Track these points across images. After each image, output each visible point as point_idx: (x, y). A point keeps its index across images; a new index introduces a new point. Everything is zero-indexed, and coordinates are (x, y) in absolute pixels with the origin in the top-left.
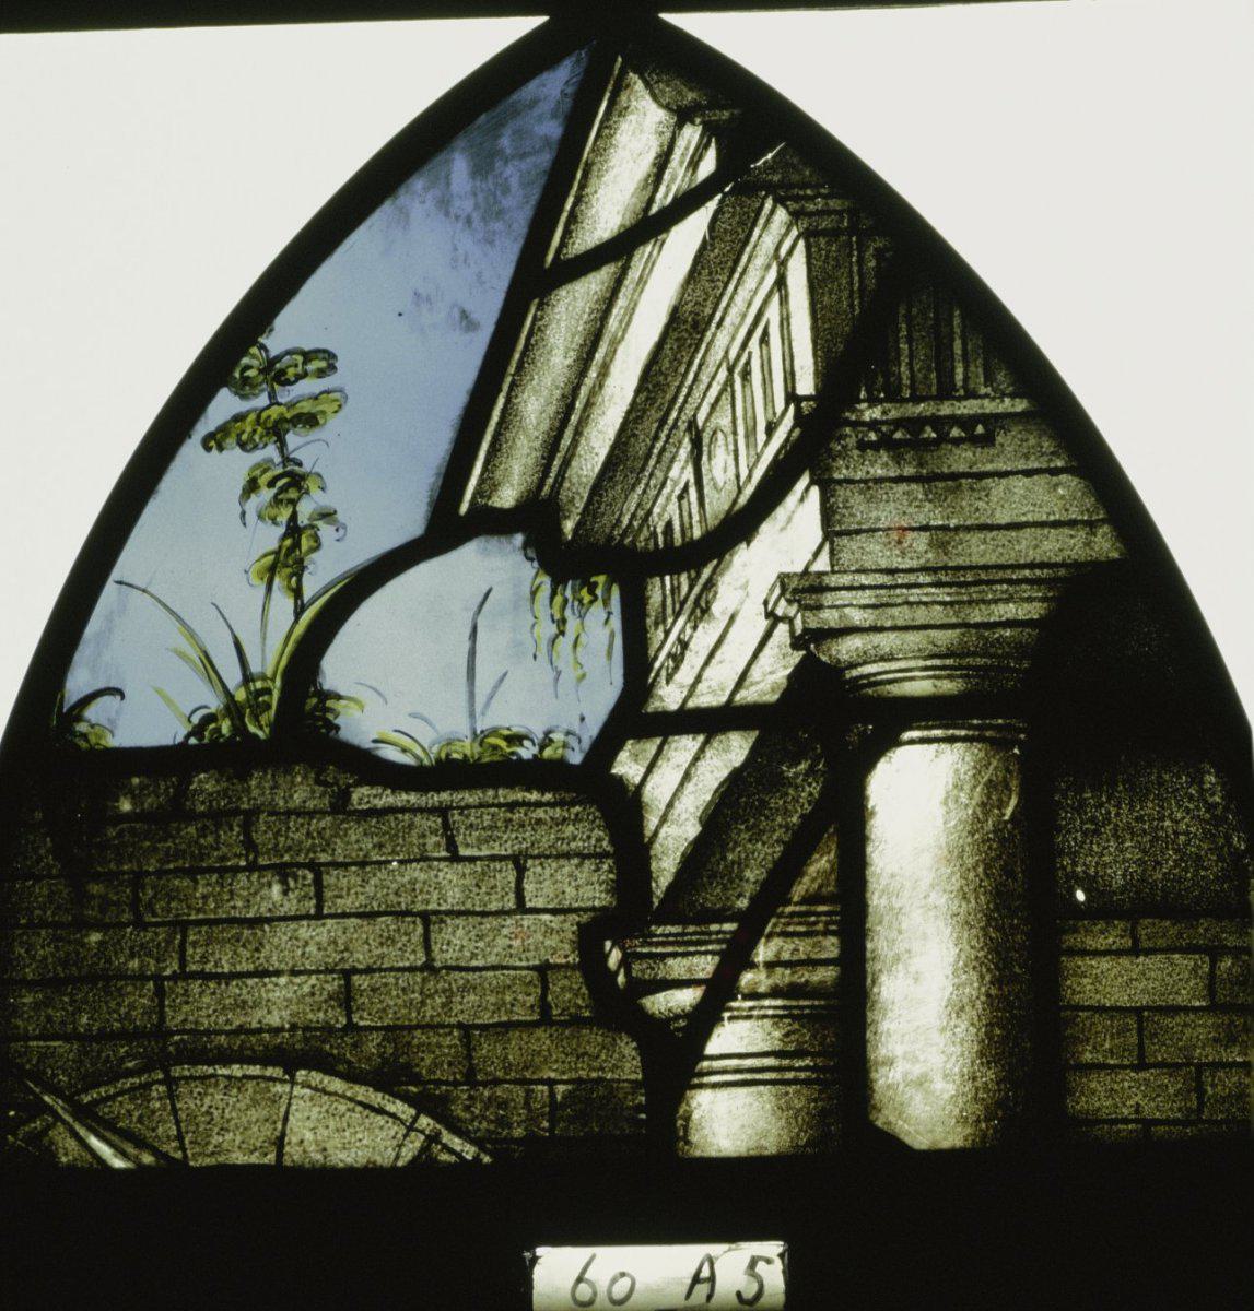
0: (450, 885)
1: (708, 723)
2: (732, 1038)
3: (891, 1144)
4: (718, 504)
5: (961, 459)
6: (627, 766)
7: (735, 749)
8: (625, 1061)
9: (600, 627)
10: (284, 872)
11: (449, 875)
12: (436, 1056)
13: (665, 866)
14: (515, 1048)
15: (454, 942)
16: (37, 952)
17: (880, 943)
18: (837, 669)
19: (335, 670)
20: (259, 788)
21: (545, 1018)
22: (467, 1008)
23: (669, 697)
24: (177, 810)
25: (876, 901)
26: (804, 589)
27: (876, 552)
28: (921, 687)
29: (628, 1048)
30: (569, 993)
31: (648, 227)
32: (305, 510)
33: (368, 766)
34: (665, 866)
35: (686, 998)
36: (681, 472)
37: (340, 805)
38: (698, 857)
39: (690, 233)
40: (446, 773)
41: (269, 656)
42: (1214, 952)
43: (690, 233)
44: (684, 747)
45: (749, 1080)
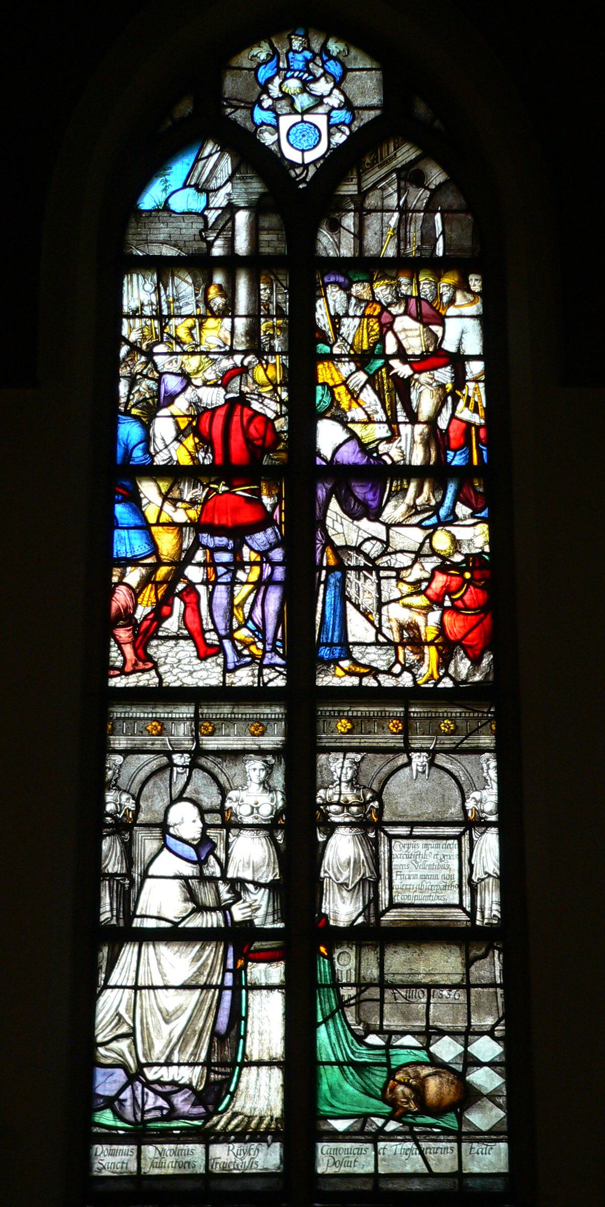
0: (184, 225)
1: (217, 209)
2: (219, 242)
3: (237, 255)
4: (218, 185)
5: (249, 181)
6: (206, 213)
7: (220, 211)
8: (204, 245)
9: (203, 197)
10: (163, 223)
11: (183, 224)
12: (181, 244)
13: (210, 224)
14: (191, 243)
15: (184, 231)
16: (132, 231)
17: (236, 233)
18: (232, 203)
19: (170, 201)
20: (160, 213)
21: (195, 240)
22: (185, 239)
23: (211, 206)
24: (150, 216)
25: (236, 228)
26: (229, 194)
27: (238, 191)
28: (243, 205)
29: (205, 244)
30: (198, 238)
31: (211, 155)
32: (167, 184)
33: (174, 212)
34: (210, 224)
35: (213, 238)
36: (214, 181)
37: (170, 216)
38: (214, 223)
39: (217, 155)
40: (183, 213)
41: (163, 200)
42: (278, 234)
43: (217, 155)
44: (213, 211)
45: (220, 247)
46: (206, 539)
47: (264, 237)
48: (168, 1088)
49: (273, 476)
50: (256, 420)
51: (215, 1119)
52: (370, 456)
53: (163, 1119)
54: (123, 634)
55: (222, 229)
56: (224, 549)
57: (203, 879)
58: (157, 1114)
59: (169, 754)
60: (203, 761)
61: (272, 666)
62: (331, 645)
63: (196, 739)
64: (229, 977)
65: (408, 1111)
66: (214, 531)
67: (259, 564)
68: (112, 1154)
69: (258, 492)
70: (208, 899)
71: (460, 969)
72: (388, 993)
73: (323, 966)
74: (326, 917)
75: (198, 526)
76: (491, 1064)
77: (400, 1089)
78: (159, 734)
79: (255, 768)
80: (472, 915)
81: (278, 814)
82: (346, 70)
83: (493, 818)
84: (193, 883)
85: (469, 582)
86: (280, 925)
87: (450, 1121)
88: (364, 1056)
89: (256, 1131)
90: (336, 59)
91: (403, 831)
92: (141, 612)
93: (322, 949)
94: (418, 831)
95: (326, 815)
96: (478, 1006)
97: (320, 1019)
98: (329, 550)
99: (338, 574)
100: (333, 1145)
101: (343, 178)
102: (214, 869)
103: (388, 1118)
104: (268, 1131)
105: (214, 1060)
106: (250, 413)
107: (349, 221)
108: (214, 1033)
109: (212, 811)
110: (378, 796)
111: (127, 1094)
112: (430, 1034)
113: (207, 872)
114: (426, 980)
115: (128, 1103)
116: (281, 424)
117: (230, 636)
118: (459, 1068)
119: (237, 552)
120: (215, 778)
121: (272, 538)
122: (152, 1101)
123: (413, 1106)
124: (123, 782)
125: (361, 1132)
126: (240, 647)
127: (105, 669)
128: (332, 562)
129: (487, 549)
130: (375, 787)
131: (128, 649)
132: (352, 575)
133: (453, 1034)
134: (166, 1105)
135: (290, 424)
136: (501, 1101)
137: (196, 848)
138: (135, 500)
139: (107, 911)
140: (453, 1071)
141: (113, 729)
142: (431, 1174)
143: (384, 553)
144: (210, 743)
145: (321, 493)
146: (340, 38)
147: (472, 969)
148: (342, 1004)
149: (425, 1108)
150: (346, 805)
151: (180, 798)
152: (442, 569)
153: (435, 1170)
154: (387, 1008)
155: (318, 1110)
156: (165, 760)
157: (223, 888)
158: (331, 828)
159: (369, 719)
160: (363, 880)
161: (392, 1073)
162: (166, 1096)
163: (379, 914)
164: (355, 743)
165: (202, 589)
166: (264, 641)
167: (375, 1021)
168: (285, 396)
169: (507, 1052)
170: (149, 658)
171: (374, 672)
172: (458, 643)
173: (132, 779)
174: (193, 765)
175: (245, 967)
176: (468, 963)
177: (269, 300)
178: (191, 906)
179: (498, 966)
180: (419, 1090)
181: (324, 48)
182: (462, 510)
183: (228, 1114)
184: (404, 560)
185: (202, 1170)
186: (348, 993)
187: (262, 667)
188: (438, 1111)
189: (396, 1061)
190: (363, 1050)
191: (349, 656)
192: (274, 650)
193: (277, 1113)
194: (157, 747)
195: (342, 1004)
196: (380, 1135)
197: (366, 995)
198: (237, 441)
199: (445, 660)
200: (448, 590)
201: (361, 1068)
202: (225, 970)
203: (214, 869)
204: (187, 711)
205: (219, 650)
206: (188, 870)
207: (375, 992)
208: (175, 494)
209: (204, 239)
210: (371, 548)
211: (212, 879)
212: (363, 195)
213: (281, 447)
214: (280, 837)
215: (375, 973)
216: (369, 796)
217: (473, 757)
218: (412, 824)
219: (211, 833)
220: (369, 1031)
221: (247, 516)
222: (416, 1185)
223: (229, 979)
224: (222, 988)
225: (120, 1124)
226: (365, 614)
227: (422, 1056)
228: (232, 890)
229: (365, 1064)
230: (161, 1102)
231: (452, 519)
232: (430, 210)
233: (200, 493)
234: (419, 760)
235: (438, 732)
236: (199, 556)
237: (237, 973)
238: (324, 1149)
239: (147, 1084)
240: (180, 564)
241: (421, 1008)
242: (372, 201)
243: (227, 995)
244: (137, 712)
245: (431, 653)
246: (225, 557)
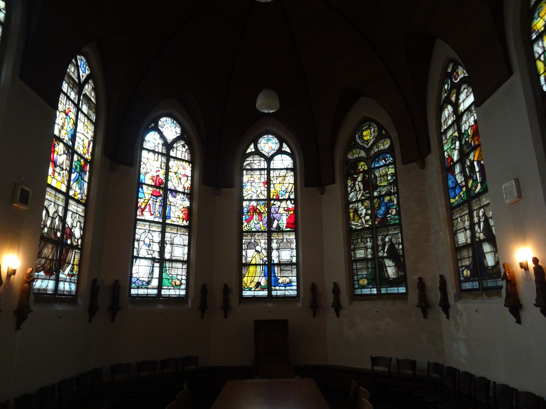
46: (152, 196)
47: (163, 150)
48: (142, 281)
49: (162, 188)
50: (160, 179)
51: (149, 286)
52: (175, 188)
53: (142, 285)
54: (140, 210)
55: (157, 147)
56: (155, 199)
57: (149, 250)
58: (141, 285)
59: (145, 230)
60: (150, 232)
61: (160, 218)
62: (168, 216)
63: (149, 228)
64: (152, 265)
65: (174, 286)
66: (154, 196)
67: (160, 202)
68: (134, 290)
69: (160, 191)
70: (150, 253)
71: (182, 266)
72: (173, 269)
73: (164, 264)
74: (165, 257)
75: (152, 195)
76: (184, 280)
77: (173, 283)
78: (144, 227)
79: (157, 233)
80: (183, 259)
81: (160, 241)
82: (176, 126)
83: (187, 245)
84: (148, 250)
85: (187, 210)
86: (159, 258)
87: (179, 287)
88: (169, 278)
89: (154, 288)
90: (175, 124)
91: (176, 245)
92: (143, 207)
93: (165, 262)
94: (178, 246)
95: (166, 242)
96: (183, 271)
97: (164, 272)
98: (169, 202)
99: (170, 206)
100: (164, 290)
101: (174, 143)
102: (150, 248)
103: (171, 286)
104: (156, 288)
105: (149, 277)
106: (159, 178)
107: (175, 150)
108: (149, 273)
109: (151, 240)
110: (173, 240)
111: (137, 282)
112: (177, 275)
113: (150, 249)
114: (177, 267)
115: (137, 283)
116: (164, 181)
117: (155, 213)
118: (181, 280)
119: (156, 199)
120: (151, 234)
121: (162, 199)
122: (140, 283)
123: (175, 285)
124: (138, 233)
125: (168, 288)
126: (156, 215)
127: (136, 215)
128: (169, 204)
129: (189, 206)
130: (173, 239)
131: (140, 212)
132: (172, 206)
133: (180, 275)
134: (142, 283)
135: (165, 181)
136: (185, 285)
137: (148, 245)
138: (142, 188)
139: (135, 254)
140: (180, 280)
141: (137, 225)
142: (176, 295)
143: (176, 204)
144: (151, 229)
145: (169, 192)
146: (176, 121)
147: (183, 266)
148: (166, 270)
149: (176, 286)
150: (169, 241)
151: (146, 237)
152: (183, 208)
153: (177, 294)
154: (172, 271)
155: (162, 285)
156: (145, 231)
157: (152, 251)
158: (167, 244)
159: (173, 228)
160: (170, 252)
161: (172, 280)
162: (142, 282)
163: (172, 257)
164: (171, 232)
165: (152, 205)
166: (159, 214)
167: (171, 273)
168: (165, 176)
169: (187, 278)
170: (143, 214)
171: (174, 221)
172: (185, 219)
173: (140, 233)
174: (149, 232)
175: (154, 264)
176: (183, 265)
177: (163, 161)
178: (147, 254)
179: (186, 266)
180: (175, 283)
181: (173, 122)
182: (187, 199)
183: (150, 285)
184: (178, 205)
185: (146, 293)
186: (167, 268)
187: (159, 218)
188: (177, 286)
189: (173, 279)
190: (169, 277)
191: (170, 218)
192: (161, 216)
193: (157, 285)
194: (144, 229)
195: (166, 270)
196: (169, 289)
197: (170, 269)
198: (157, 182)
199: (183, 221)
200: (184, 211)
201: (168, 279)
202: (151, 264)
203: (150, 248)
204: (148, 224)
205: (153, 215)
206: (148, 248)
207: (171, 269)
208: (148, 189)
209: (155, 148)
210: (175, 203)
211: (150, 250)
212: (177, 147)
213: (164, 184)
214: (160, 245)
215: (171, 266)
216: (172, 240)
217: (185, 236)
218: (177, 245)
219: (151, 243)
220: (170, 274)
221: (158, 194)
222: (174, 296)
223: (152, 266)
224: (151, 266)
225: (136, 286)
226: (173, 213)
227: (176, 278)
228: (153, 252)
229: (169, 279)
230: (142, 283)
231: (185, 201)
232: (185, 152)
233: (152, 189)
234: (179, 235)
235: (181, 232)
236: (152, 199)
237: (153, 265)
238: (163, 290)
239: (140, 280)
240: (149, 200)
241: (176, 271)
242: (178, 148)
243: (152, 267)
244: (141, 223)
245: (181, 220)
246: (155, 200)
